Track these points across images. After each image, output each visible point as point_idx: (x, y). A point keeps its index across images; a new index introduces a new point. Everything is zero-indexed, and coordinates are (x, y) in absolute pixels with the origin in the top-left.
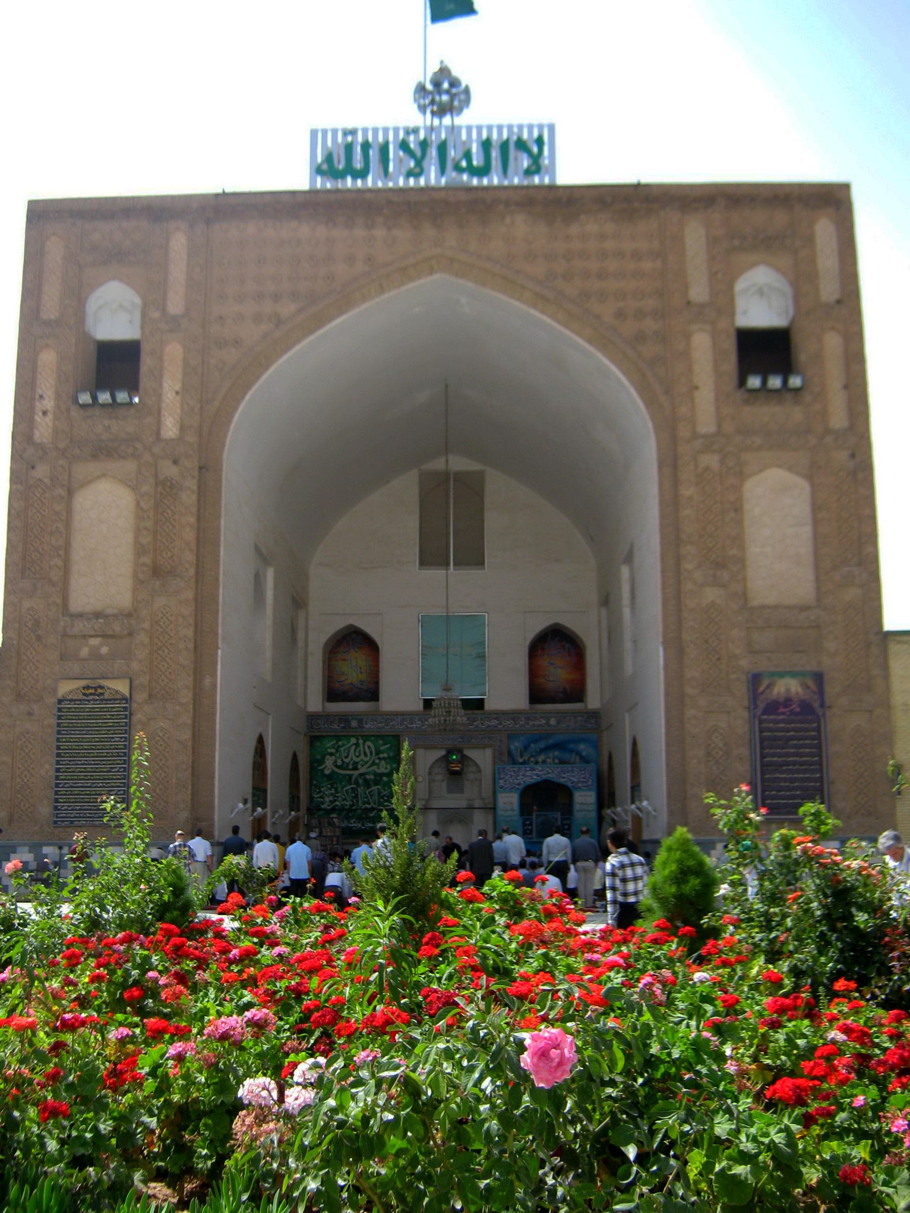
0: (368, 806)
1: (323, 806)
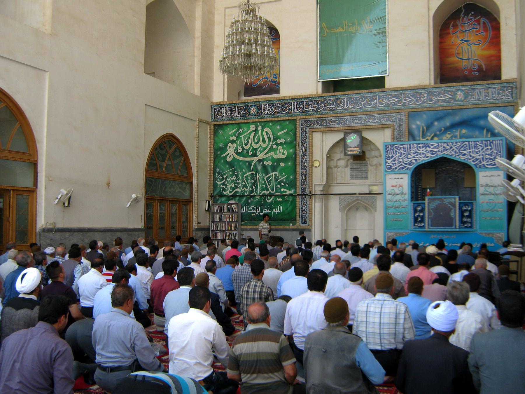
0: (267, 193)
1: (225, 193)
